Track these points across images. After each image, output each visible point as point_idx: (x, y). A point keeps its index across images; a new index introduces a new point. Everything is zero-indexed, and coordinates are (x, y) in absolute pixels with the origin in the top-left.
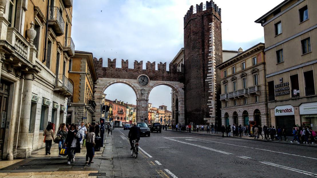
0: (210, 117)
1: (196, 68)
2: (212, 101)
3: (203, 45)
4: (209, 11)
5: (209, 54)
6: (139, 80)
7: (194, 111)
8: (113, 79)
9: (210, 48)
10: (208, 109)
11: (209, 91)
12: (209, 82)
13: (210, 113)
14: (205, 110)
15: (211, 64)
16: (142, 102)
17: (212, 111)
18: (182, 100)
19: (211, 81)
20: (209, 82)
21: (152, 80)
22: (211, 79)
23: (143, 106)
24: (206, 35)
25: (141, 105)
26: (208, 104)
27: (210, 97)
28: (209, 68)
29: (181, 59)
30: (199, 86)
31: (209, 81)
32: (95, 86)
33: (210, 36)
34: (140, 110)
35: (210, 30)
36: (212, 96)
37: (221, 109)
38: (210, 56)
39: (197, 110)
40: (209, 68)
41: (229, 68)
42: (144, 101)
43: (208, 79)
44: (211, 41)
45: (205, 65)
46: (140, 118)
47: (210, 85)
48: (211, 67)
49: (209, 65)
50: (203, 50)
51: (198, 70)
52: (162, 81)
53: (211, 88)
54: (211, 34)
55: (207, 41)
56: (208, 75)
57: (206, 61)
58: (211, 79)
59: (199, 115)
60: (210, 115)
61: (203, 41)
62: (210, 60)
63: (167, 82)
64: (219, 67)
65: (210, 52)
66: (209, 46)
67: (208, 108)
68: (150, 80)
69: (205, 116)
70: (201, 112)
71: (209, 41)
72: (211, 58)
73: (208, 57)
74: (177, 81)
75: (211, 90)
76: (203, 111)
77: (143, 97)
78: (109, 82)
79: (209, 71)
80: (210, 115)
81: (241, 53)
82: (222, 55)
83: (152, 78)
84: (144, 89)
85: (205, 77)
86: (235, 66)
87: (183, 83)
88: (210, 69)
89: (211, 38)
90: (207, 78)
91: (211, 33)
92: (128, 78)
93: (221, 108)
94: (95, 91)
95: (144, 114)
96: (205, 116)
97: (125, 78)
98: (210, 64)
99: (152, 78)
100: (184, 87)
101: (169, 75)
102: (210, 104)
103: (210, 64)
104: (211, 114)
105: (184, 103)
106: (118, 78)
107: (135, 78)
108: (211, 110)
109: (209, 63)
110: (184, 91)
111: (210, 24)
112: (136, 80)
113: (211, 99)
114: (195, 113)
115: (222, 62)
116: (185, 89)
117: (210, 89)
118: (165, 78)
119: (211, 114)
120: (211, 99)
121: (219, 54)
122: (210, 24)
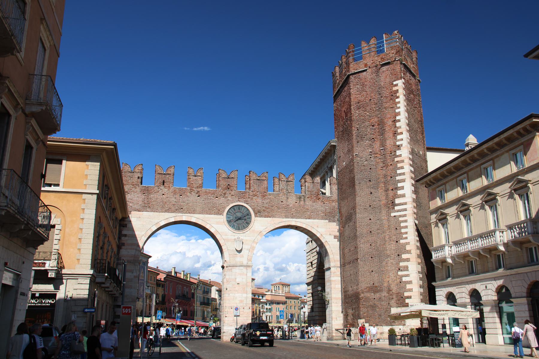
0: (407, 305)
1: (368, 183)
3: (382, 133)
4: (391, 55)
5: (398, 153)
6: (229, 216)
7: (366, 292)
9: (399, 137)
10: (402, 284)
11: (402, 241)
12: (401, 219)
13: (406, 294)
14: (394, 289)
15: (404, 174)
17: (411, 290)
19: (405, 216)
20: (401, 219)
21: (261, 216)
22: (405, 210)
23: (238, 280)
24: (385, 108)
26: (400, 273)
27: (404, 256)
28: (400, 185)
29: (329, 166)
31: (400, 216)
32: (124, 232)
33: (397, 111)
36: (409, 252)
37: (433, 284)
38: (400, 156)
40: (400, 185)
41: (450, 183)
44: (399, 121)
45: (389, 178)
46: (232, 310)
47: (402, 225)
48: (405, 181)
49: (398, 178)
50: (383, 145)
51: (372, 191)
52: (285, 219)
53: (406, 233)
54: (398, 105)
55: (390, 122)
56: (397, 201)
57: (391, 167)
58: (405, 210)
60: (407, 301)
61: (381, 123)
62: (399, 165)
64: (426, 182)
65: (399, 147)
66: (395, 134)
68: (256, 216)
69: (393, 302)
70: (384, 294)
71: (395, 121)
72: (403, 161)
73: (396, 159)
75: (406, 238)
76: (389, 290)
78: (156, 221)
80: (407, 301)
81: (473, 146)
82: (425, 155)
84: (241, 238)
86: (465, 175)
88: (402, 188)
89: (399, 114)
90: (397, 208)
91: (399, 102)
93: (435, 281)
94: (123, 244)
95: (241, 301)
96: (393, 302)
97: (194, 212)
98: (400, 174)
99: (258, 213)
100: (338, 234)
101: (302, 203)
103: (400, 174)
104: (409, 297)
106: (179, 212)
107: (219, 212)
108: (408, 286)
109: (399, 172)
111: (395, 83)
113: (408, 260)
114: (368, 295)
115: (427, 171)
117: (404, 236)
118: (293, 210)
119: (409, 297)
120: (408, 260)
121: (419, 152)
122: (395, 83)
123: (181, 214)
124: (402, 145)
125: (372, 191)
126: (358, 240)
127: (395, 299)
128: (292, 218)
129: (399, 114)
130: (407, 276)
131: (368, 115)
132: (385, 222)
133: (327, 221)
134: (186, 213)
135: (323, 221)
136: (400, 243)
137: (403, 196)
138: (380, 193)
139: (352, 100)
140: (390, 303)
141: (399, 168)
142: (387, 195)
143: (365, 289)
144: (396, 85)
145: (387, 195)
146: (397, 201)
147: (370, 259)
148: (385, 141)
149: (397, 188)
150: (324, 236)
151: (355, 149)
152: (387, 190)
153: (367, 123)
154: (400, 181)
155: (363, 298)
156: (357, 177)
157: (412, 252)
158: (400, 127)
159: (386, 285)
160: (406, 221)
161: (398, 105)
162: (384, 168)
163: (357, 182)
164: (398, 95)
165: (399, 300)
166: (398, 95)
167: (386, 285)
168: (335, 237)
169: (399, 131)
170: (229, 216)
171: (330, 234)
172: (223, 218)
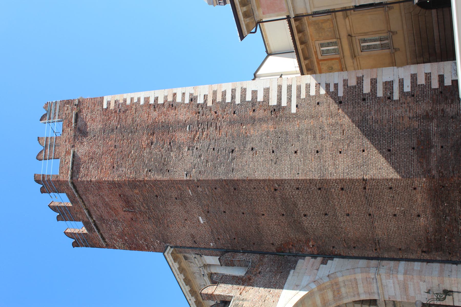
2: (384, 81)
3: (166, 128)
5: (200, 100)
7: (428, 164)
10: (418, 92)
12: (303, 96)
13: (435, 85)
14: (424, 107)
15: (233, 91)
17: (428, 76)
18: (373, 270)
19: (299, 88)
20: (303, 96)
22: (289, 88)
26: (396, 96)
27: (367, 89)
28: (249, 98)
30: (315, 137)
31: (298, 96)
33: (142, 102)
35: (122, 104)
36: (360, 80)
39: (423, 147)
43: (289, 100)
44: (156, 99)
48: (245, 89)
49: (238, 101)
54: (135, 100)
55: (155, 114)
58: (289, 88)
59: (444, 135)
60: (448, 82)
62: (219, 99)
65: (193, 99)
66: (172, 105)
70: (433, 126)
71: (156, 106)
73: (210, 104)
75: (336, 85)
76: (427, 117)
79: (260, 98)
80: (448, 82)
88: (254, 93)
89: (147, 99)
90: (284, 103)
98: (233, 97)
100: (319, 259)
103: (233, 97)
104: (441, 78)
105: (392, 263)
108: (421, 81)
109: (228, 100)
110: (336, 260)
113: (374, 82)
114: (434, 160)
116: (326, 255)
119: (441, 78)
120: (374, 82)
122: (105, 106)
124: (191, 94)
125: (249, 147)
126: (329, 177)
127: (443, 106)
129: (147, 99)
130: (401, 83)
131: (136, 152)
132: (306, 124)
135: (290, 277)
138: (255, 132)
139: (106, 179)
140: (451, 114)
142: (261, 120)
143: (422, 166)
144: (109, 103)
145: (261, 120)
146: (273, 102)
147: (365, 154)
149: (254, 102)
150: (317, 277)
151: (177, 177)
152: (253, 120)
155: (439, 172)
156: (221, 174)
157: (361, 75)
158: (166, 97)
159: (415, 124)
161: (135, 100)
162: (219, 124)
163: (231, 176)
165: (446, 99)
166: (121, 101)
167: (415, 124)
168: (324, 263)
171: (318, 270)
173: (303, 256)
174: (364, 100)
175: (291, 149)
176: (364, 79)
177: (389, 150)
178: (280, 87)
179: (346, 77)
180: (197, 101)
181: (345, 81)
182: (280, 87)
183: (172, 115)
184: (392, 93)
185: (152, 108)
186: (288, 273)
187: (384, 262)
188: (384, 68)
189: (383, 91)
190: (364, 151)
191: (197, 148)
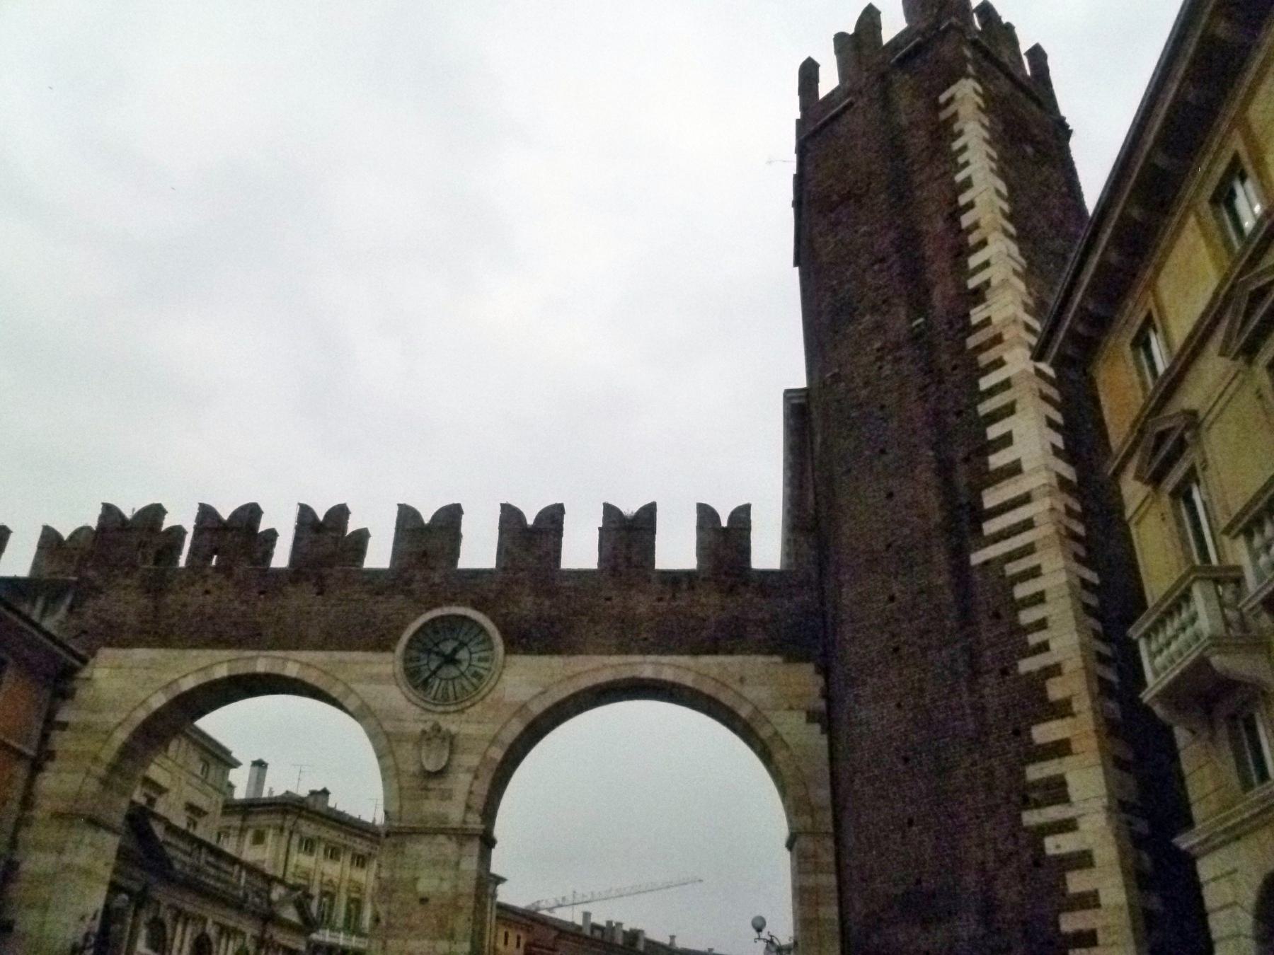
2: (1070, 778)
5: (977, 315)
8: (203, 657)
11: (1028, 665)
12: (1013, 568)
15: (1006, 385)
16: (421, 849)
17: (1089, 901)
20: (1013, 568)
21: (528, 650)
22: (1028, 525)
23: (424, 886)
25: (406, 874)
26: (1031, 818)
27: (1044, 733)
28: (994, 432)
31: (1010, 557)
32: (62, 716)
33: (959, 177)
34: (390, 925)
36: (1062, 710)
38: (987, 322)
40: (994, 432)
42: (441, 839)
47: (1021, 591)
49: (985, 408)
50: (919, 305)
51: (893, 484)
52: (615, 659)
53: (1042, 625)
56: (991, 499)
58: (1028, 525)
61: (909, 241)
63: (665, 659)
65: (978, 296)
66: (961, 251)
67: (1039, 859)
68: (507, 652)
71: (956, 213)
72: (997, 340)
73: (972, 342)
74: (758, 652)
75: (1044, 647)
76: (989, 909)
77: (431, 807)
78: (169, 677)
83: (526, 635)
85: (966, 519)
87: (809, 668)
88: (1006, 440)
90: (990, 527)
92: (327, 642)
94: (51, 756)
97: (297, 642)
98: (991, 392)
100: (821, 704)
102: (1053, 813)
103: (991, 392)
105: (828, 859)
108: (1077, 882)
109: (985, 383)
110: (824, 741)
111: (943, 98)
112: (388, 656)
113: (1061, 749)
117: (1034, 639)
120: (1061, 749)
122: (943, 98)
123: (254, 653)
124: (987, 283)
125: (893, 484)
128: (644, 651)
129: (967, 184)
130: (1067, 826)
133: (777, 659)
134: (270, 648)
135: (761, 659)
136: (1018, 678)
137: (1014, 470)
141: (986, 371)
148: (927, 292)
153: (863, 261)
154: (994, 417)
157: (1076, 707)
160: (1035, 573)
164: (956, 127)
168: (812, 717)
169: (973, 239)
170: (414, 653)
171: (791, 708)
172: (388, 663)
173: (825, 670)
174: (1017, 733)
175: (896, 588)
176: (1069, 720)
177: (911, 823)
178: (1026, 499)
179: (1068, 668)
180: (976, 304)
181: (1054, 671)
182: (1026, 499)
183: (939, 266)
184: (1038, 805)
185: (951, 210)
186: (771, 653)
187: (830, 843)
188: (1100, 770)
189: (1040, 781)
190: (906, 760)
191: (880, 368)
